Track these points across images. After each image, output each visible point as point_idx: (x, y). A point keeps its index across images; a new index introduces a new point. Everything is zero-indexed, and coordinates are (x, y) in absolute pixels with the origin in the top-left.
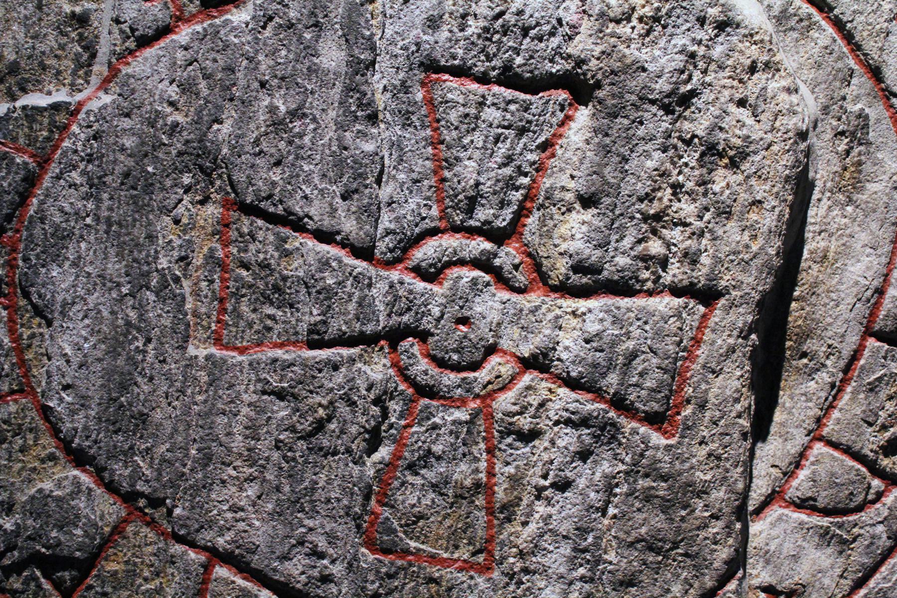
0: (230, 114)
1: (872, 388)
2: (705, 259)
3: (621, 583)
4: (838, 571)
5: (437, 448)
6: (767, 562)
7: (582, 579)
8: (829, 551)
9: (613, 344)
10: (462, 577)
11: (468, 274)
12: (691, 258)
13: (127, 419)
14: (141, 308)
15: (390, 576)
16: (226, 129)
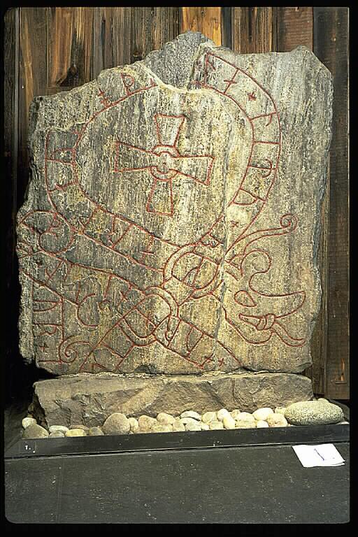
0: (117, 124)
1: (250, 177)
2: (211, 149)
5: (160, 190)
11: (165, 154)
12: (209, 149)
13: (97, 186)
14: (100, 163)
16: (116, 127)
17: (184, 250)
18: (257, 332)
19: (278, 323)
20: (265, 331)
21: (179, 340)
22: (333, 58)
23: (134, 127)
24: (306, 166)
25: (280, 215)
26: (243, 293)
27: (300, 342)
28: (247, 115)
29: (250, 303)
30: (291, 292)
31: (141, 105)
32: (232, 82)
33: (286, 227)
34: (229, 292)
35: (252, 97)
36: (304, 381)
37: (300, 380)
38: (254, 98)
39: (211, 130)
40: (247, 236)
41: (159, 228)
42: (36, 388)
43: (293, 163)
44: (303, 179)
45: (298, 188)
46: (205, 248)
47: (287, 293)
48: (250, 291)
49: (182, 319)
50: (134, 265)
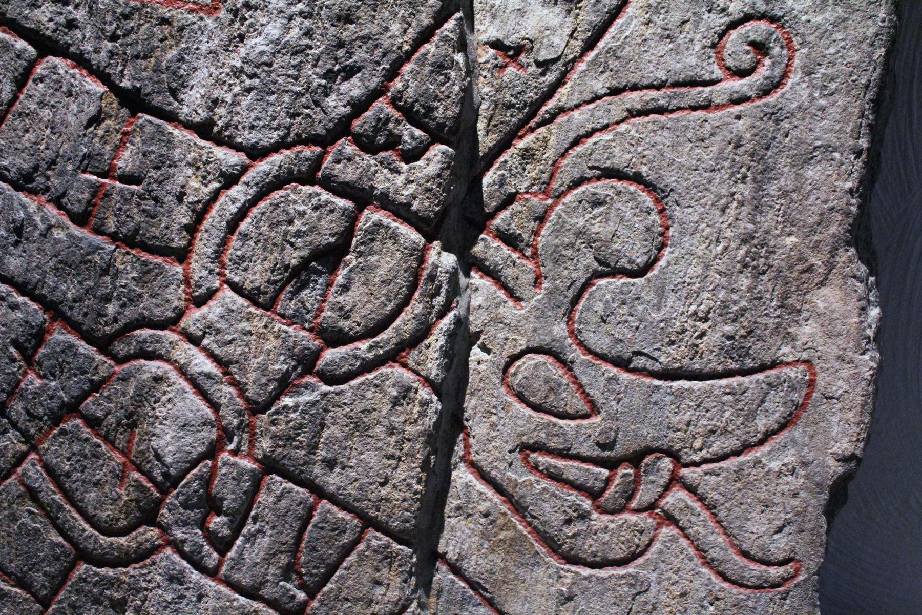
3: (339, 18)
4: (568, 31)
6: (494, 17)
7: (301, 13)
8: (557, 9)
10: (191, 18)
15: (126, 17)
17: (263, 166)
18: (599, 520)
19: (692, 489)
20: (633, 518)
25: (718, 21)
26: (540, 358)
27: (775, 572)
30: (749, 363)
33: (742, 73)
34: (484, 356)
40: (561, 110)
41: (157, 70)
46: (368, 160)
47: (734, 366)
49: (269, 465)
50: (58, 234)
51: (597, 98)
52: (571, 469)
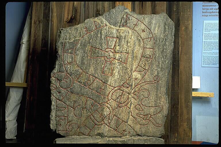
0: (91, 40)
1: (142, 61)
2: (128, 50)
9: (121, 56)
11: (109, 52)
12: (126, 50)
13: (83, 63)
16: (91, 41)
17: (116, 89)
18: (143, 121)
21: (113, 123)
22: (174, 20)
23: (98, 41)
24: (164, 58)
25: (153, 76)
27: (160, 125)
28: (141, 38)
29: (141, 109)
31: (101, 33)
32: (136, 25)
35: (143, 31)
36: (161, 140)
37: (160, 140)
38: (145, 31)
39: (128, 43)
41: (106, 80)
42: (57, 141)
43: (158, 57)
44: (163, 63)
45: (160, 66)
47: (155, 106)
48: (141, 105)
49: (114, 115)
51: (143, 83)
52: (141, 116)
